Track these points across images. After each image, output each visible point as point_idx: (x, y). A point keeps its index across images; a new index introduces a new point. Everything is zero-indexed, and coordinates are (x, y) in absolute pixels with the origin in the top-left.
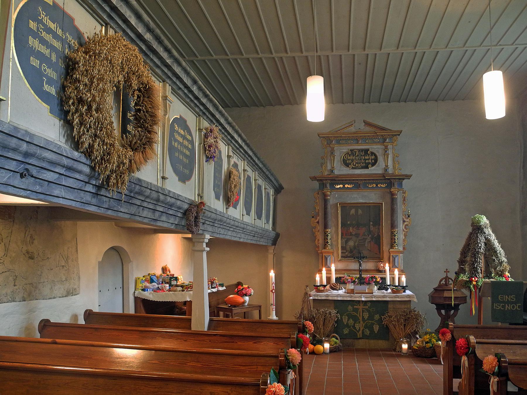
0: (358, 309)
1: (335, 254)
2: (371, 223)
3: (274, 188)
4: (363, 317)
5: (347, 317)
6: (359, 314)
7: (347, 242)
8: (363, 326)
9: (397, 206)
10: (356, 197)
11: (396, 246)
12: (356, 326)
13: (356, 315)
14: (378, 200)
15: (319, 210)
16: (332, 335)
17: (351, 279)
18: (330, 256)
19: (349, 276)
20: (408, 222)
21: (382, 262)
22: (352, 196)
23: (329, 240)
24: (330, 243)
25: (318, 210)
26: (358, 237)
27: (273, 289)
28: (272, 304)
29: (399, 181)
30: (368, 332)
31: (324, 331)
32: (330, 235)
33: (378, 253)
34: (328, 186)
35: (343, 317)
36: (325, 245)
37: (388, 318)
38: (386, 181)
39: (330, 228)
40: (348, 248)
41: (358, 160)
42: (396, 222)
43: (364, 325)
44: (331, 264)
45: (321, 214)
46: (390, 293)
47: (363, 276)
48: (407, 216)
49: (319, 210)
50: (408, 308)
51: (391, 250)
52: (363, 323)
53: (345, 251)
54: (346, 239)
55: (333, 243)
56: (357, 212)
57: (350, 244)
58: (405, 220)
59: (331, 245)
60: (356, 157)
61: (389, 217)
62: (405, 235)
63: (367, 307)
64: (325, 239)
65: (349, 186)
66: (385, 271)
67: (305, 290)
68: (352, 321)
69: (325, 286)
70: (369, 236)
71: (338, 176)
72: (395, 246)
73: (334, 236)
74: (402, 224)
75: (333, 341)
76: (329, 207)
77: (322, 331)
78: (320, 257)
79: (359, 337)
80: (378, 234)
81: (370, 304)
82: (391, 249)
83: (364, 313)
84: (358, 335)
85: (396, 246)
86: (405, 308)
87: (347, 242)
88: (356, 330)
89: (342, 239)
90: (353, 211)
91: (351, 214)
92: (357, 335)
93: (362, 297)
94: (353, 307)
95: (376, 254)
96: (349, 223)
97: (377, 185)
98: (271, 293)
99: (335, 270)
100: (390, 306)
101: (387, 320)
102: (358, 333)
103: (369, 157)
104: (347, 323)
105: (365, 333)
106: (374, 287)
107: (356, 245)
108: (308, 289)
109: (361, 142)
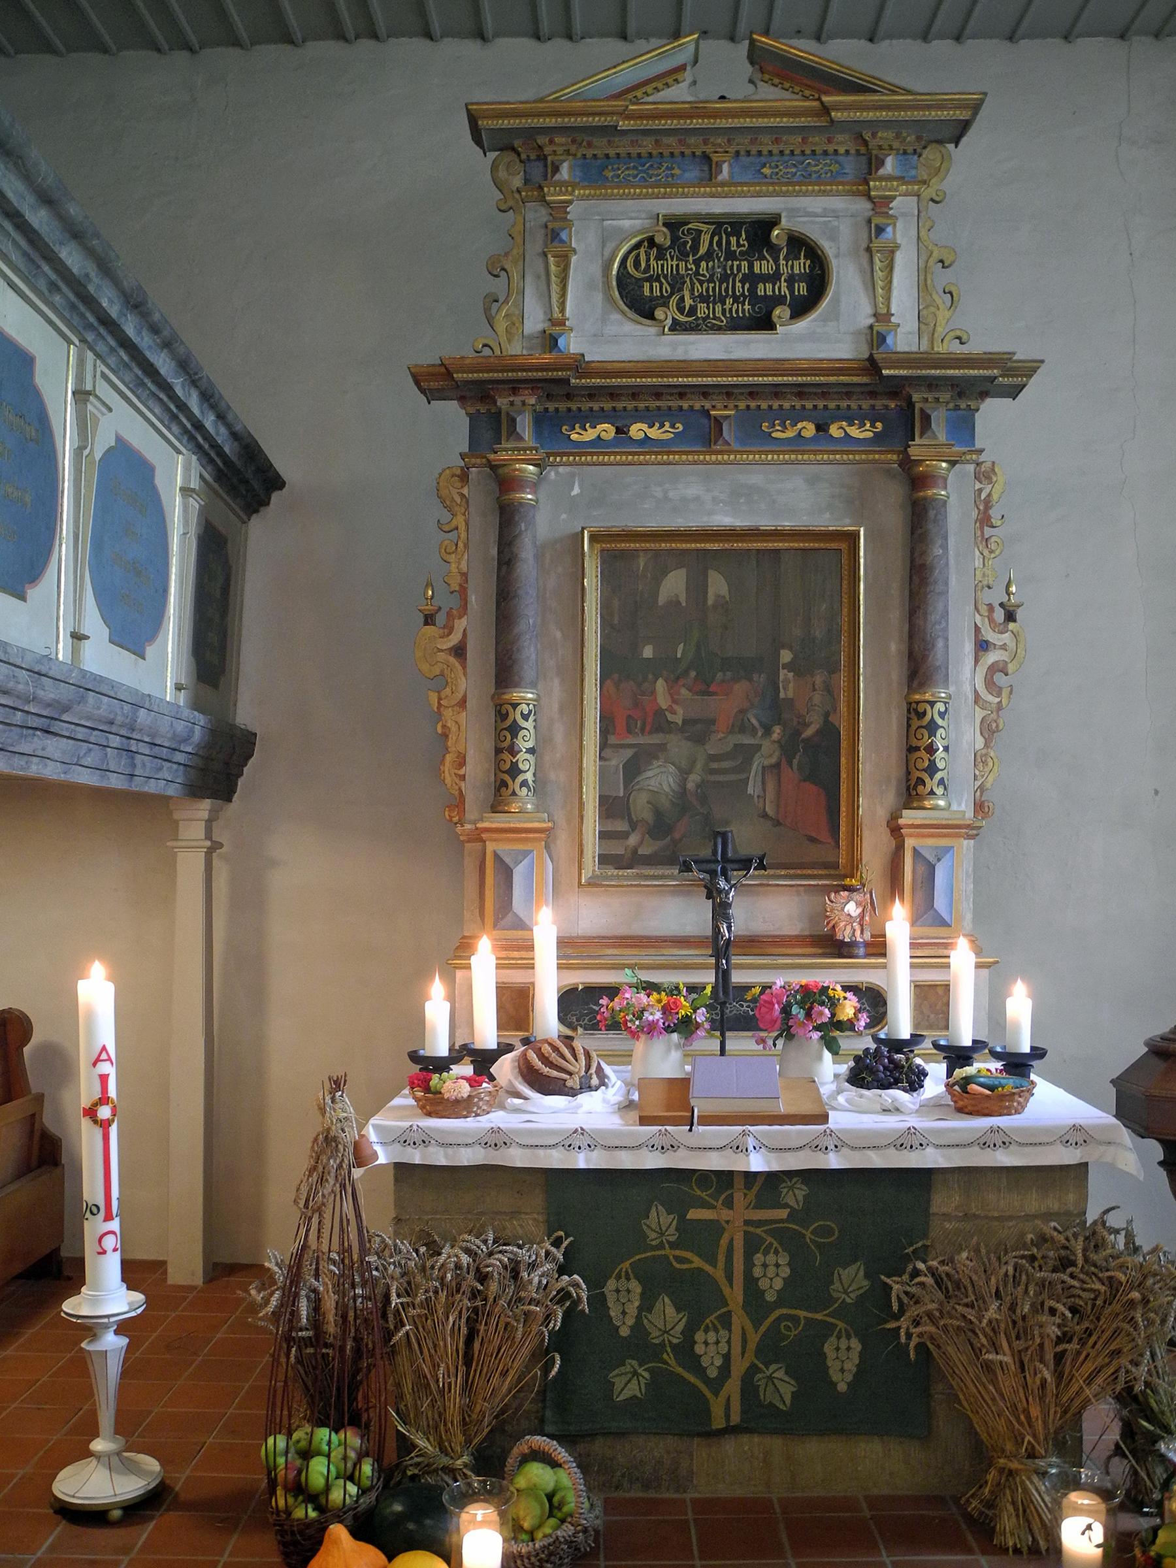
0: (715, 1229)
1: (563, 843)
2: (786, 656)
3: (200, 446)
4: (750, 1281)
5: (636, 1287)
6: (721, 1258)
7: (632, 770)
8: (752, 1345)
9: (945, 547)
10: (697, 499)
11: (939, 791)
12: (699, 1349)
13: (700, 1270)
14: (827, 515)
15: (465, 575)
16: (521, 1447)
17: (666, 1010)
18: (526, 853)
19: (650, 988)
20: (1004, 647)
21: (850, 889)
22: (671, 494)
23: (522, 756)
24: (529, 776)
25: (458, 579)
26: (700, 739)
27: (104, 1100)
28: (94, 1210)
29: (957, 408)
30: (787, 1389)
31: (470, 1407)
32: (529, 725)
33: (824, 836)
34: (525, 426)
35: (611, 1284)
36: (498, 789)
37: (940, 1295)
38: (879, 403)
39: (533, 685)
40: (641, 806)
41: (709, 281)
42: (940, 644)
43: (754, 1339)
44: (532, 901)
45: (480, 599)
46: (933, 1106)
47: (737, 977)
48: (999, 615)
49: (465, 575)
50: (1068, 1213)
51: (909, 817)
52: (749, 1326)
53: (621, 826)
54: (629, 753)
55: (552, 776)
56: (697, 587)
57: (653, 784)
58: (990, 635)
59: (540, 787)
60: (697, 263)
61: (896, 616)
62: (989, 730)
63: (783, 1214)
64: (498, 751)
65: (654, 433)
66: (878, 947)
67: (323, 1111)
68: (670, 1311)
69: (484, 1061)
70: (768, 731)
71: (579, 365)
72: (932, 793)
73: (559, 735)
74: (969, 660)
75: (532, 1490)
76: (527, 552)
77: (455, 1402)
78: (470, 865)
79: (718, 1423)
80: (826, 722)
81: (800, 1194)
82: (906, 813)
83: (758, 1258)
84: (717, 1411)
85: (939, 791)
86: (1048, 1216)
87: (632, 770)
88: (700, 1371)
89: (608, 752)
90: (674, 585)
91: (662, 600)
92: (707, 1412)
93: (751, 1143)
94: (682, 1218)
95: (812, 840)
96: (648, 652)
97: (821, 428)
98: (86, 1123)
99: (565, 944)
100: (943, 1202)
101: (929, 1315)
102: (716, 1394)
103: (776, 260)
104: (638, 1327)
105: (767, 1396)
106: (820, 1058)
107: (690, 785)
108: (346, 1106)
109: (731, 174)
